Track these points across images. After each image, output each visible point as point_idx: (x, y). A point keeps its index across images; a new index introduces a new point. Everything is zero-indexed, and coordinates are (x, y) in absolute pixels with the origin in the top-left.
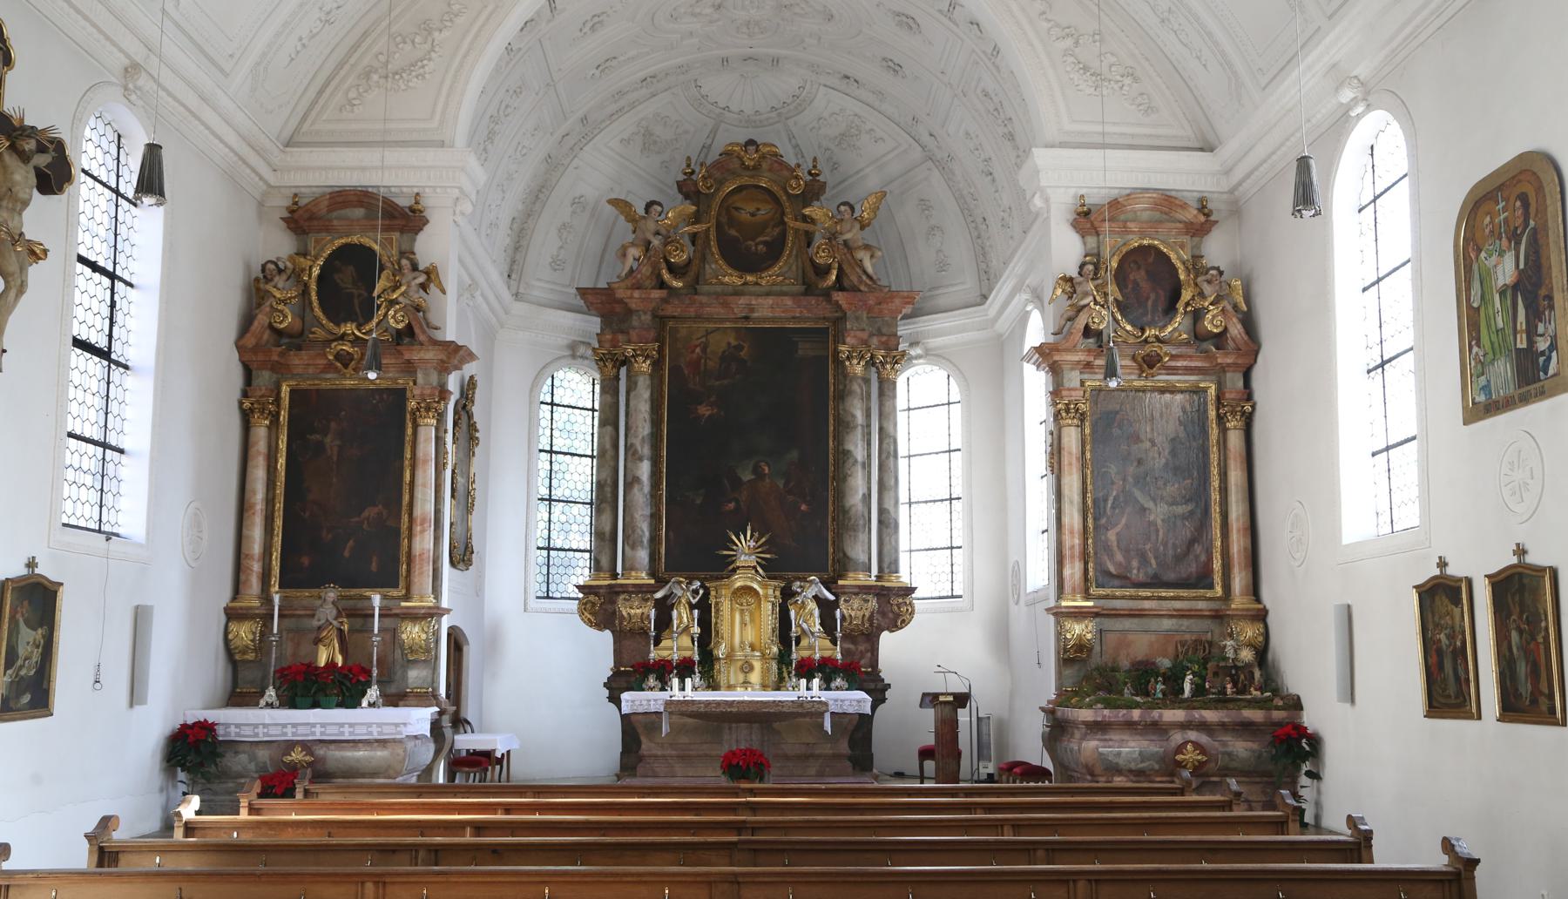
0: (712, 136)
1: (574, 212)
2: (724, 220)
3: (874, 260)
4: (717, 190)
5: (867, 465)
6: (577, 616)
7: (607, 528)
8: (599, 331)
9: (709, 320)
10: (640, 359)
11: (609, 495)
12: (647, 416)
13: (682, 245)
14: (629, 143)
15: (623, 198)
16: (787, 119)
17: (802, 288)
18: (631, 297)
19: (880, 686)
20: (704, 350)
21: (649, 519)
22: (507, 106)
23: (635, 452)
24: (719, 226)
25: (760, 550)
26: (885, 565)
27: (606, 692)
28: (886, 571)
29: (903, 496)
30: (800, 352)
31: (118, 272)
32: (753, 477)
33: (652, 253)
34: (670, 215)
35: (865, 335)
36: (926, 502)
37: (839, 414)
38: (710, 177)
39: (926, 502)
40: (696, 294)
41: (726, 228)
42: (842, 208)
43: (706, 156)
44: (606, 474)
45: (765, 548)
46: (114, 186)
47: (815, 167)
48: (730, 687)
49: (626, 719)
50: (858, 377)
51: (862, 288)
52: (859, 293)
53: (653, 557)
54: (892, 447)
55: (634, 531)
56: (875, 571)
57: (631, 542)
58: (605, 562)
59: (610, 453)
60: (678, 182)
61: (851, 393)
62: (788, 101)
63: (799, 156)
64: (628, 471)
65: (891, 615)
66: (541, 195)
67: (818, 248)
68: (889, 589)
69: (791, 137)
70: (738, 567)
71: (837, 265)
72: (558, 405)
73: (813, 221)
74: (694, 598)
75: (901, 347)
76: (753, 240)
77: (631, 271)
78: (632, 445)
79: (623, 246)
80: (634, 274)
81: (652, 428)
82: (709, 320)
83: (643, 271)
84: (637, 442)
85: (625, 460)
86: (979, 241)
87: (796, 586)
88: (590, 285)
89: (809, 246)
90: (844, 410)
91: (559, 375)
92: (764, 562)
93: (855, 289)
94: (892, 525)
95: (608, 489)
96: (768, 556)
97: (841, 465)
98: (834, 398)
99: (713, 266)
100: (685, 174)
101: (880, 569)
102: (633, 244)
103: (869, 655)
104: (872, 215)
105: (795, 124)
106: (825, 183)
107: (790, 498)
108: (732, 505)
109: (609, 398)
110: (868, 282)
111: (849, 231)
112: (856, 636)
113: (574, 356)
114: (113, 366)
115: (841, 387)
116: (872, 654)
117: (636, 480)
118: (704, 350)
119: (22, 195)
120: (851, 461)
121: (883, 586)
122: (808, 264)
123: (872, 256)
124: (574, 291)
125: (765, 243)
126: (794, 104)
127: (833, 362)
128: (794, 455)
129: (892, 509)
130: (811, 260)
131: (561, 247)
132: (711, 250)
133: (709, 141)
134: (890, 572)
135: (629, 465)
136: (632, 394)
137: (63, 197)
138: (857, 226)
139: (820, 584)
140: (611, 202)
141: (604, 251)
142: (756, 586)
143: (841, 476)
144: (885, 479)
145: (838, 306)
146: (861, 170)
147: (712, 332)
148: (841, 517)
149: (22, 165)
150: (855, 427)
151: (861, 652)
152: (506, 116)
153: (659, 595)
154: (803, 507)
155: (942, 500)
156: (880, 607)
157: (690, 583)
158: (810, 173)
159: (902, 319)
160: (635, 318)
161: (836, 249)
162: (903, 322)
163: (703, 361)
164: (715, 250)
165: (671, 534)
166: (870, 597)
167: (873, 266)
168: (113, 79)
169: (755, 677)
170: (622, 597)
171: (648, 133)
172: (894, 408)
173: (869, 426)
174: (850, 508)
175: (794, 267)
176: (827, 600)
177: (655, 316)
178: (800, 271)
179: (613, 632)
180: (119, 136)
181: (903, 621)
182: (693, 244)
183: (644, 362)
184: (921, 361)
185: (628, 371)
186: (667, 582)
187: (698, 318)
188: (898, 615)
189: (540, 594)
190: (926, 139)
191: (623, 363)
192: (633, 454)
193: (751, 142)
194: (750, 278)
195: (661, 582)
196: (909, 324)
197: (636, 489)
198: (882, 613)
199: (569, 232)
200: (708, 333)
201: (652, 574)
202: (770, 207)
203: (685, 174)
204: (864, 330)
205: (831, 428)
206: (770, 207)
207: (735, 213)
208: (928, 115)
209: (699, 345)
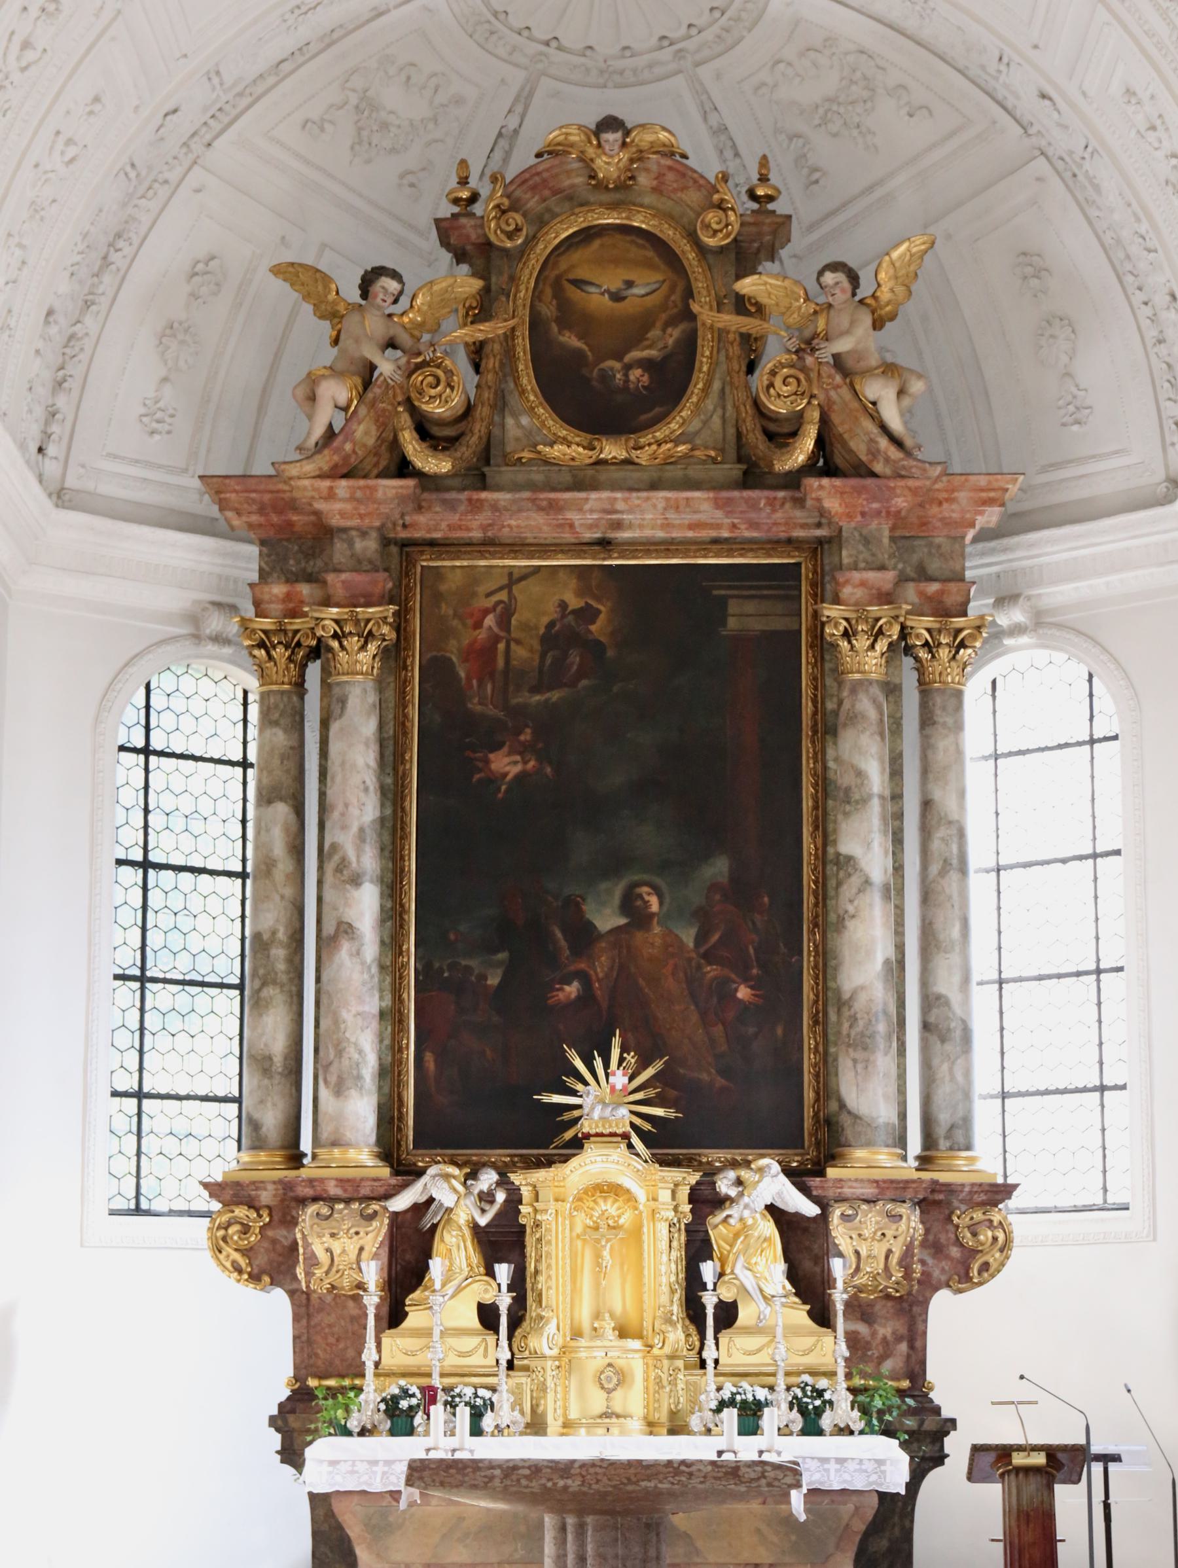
0: (519, 109)
1: (194, 296)
2: (548, 310)
3: (906, 401)
4: (531, 240)
5: (894, 891)
6: (208, 1254)
7: (278, 1045)
8: (254, 577)
9: (517, 548)
10: (353, 642)
11: (281, 966)
12: (371, 780)
13: (449, 373)
14: (322, 130)
15: (309, 260)
16: (698, 64)
17: (735, 471)
18: (331, 495)
19: (930, 1424)
20: (504, 621)
21: (375, 1024)
22: (26, 45)
23: (343, 865)
24: (536, 325)
25: (639, 1096)
26: (940, 1131)
27: (275, 1440)
28: (943, 1144)
29: (982, 964)
30: (732, 623)
32: (622, 921)
33: (377, 391)
34: (419, 301)
35: (885, 579)
36: (1040, 978)
37: (825, 768)
38: (515, 206)
39: (1040, 978)
40: (484, 487)
41: (555, 328)
42: (829, 278)
43: (506, 160)
44: (274, 918)
45: (651, 1093)
47: (764, 179)
48: (568, 1426)
49: (319, 1502)
50: (870, 682)
51: (878, 467)
52: (869, 482)
53: (388, 1118)
54: (955, 848)
55: (340, 1053)
56: (915, 1145)
57: (333, 1079)
58: (271, 1119)
59: (284, 865)
60: (438, 222)
61: (854, 718)
62: (700, 22)
63: (729, 154)
64: (326, 909)
65: (955, 1252)
66: (114, 257)
67: (773, 373)
68: (949, 1188)
69: (708, 109)
70: (587, 1136)
71: (816, 415)
72: (161, 754)
73: (759, 310)
74: (483, 1211)
75: (974, 609)
76: (619, 357)
77: (330, 434)
78: (334, 847)
79: (309, 374)
80: (336, 443)
81: (382, 805)
82: (517, 548)
84: (345, 840)
85: (320, 883)
86: (1163, 349)
87: (725, 1185)
88: (238, 471)
89: (751, 368)
90: (836, 759)
91: (163, 682)
92: (647, 1126)
93: (863, 471)
94: (957, 1034)
95: (279, 954)
96: (659, 1112)
97: (831, 893)
98: (815, 732)
99: (525, 420)
100: (456, 201)
101: (929, 1140)
102: (334, 371)
103: (903, 1347)
104: (900, 290)
105: (718, 76)
106: (789, 217)
107: (711, 971)
108: (572, 990)
109: (280, 738)
110: (894, 453)
111: (847, 332)
112: (871, 1304)
113: (197, 638)
115: (830, 705)
116: (912, 1347)
117: (346, 929)
118: (504, 621)
120: (855, 881)
121: (935, 1182)
122: (748, 411)
123: (901, 393)
124: (197, 483)
125: (647, 365)
126: (715, 29)
127: (812, 646)
128: (718, 868)
129: (954, 997)
130: (757, 404)
131: (165, 380)
132: (517, 380)
133: (513, 123)
134: (951, 1149)
135: (328, 895)
136: (335, 727)
138: (867, 320)
139: (783, 1178)
140: (278, 270)
141: (265, 392)
142: (628, 1182)
143: (832, 917)
144: (938, 925)
145: (822, 512)
146: (880, 183)
147: (523, 578)
148: (833, 1017)
150: (865, 801)
151: (885, 1339)
152: (24, 69)
153: (401, 1203)
154: (743, 993)
155: (1078, 974)
156: (927, 1231)
157: (473, 1175)
158: (752, 195)
159: (976, 540)
160: (339, 546)
161: (813, 375)
162: (980, 546)
163: (501, 646)
164: (528, 380)
165: (429, 1058)
166: (903, 1209)
167: (906, 414)
169: (633, 1400)
170: (312, 1209)
171: (367, 105)
172: (959, 753)
173: (897, 797)
174: (855, 993)
175: (716, 421)
176: (797, 1215)
177: (386, 542)
178: (731, 431)
179: (292, 1294)
181: (985, 1266)
182: (477, 368)
183: (363, 648)
184: (1024, 640)
185: (326, 672)
186: (420, 1173)
187: (490, 545)
188: (974, 1252)
189: (121, 1204)
190: (1028, 105)
191: (316, 652)
192: (339, 870)
193: (610, 123)
194: (612, 450)
195: (408, 1173)
196: (992, 552)
197: (344, 952)
198: (933, 1245)
199: (182, 342)
200: (514, 579)
201: (388, 1150)
202: (659, 277)
203: (456, 201)
204: (882, 568)
205: (807, 804)
206: (659, 277)
207: (573, 293)
208: (1036, 47)
209: (494, 609)
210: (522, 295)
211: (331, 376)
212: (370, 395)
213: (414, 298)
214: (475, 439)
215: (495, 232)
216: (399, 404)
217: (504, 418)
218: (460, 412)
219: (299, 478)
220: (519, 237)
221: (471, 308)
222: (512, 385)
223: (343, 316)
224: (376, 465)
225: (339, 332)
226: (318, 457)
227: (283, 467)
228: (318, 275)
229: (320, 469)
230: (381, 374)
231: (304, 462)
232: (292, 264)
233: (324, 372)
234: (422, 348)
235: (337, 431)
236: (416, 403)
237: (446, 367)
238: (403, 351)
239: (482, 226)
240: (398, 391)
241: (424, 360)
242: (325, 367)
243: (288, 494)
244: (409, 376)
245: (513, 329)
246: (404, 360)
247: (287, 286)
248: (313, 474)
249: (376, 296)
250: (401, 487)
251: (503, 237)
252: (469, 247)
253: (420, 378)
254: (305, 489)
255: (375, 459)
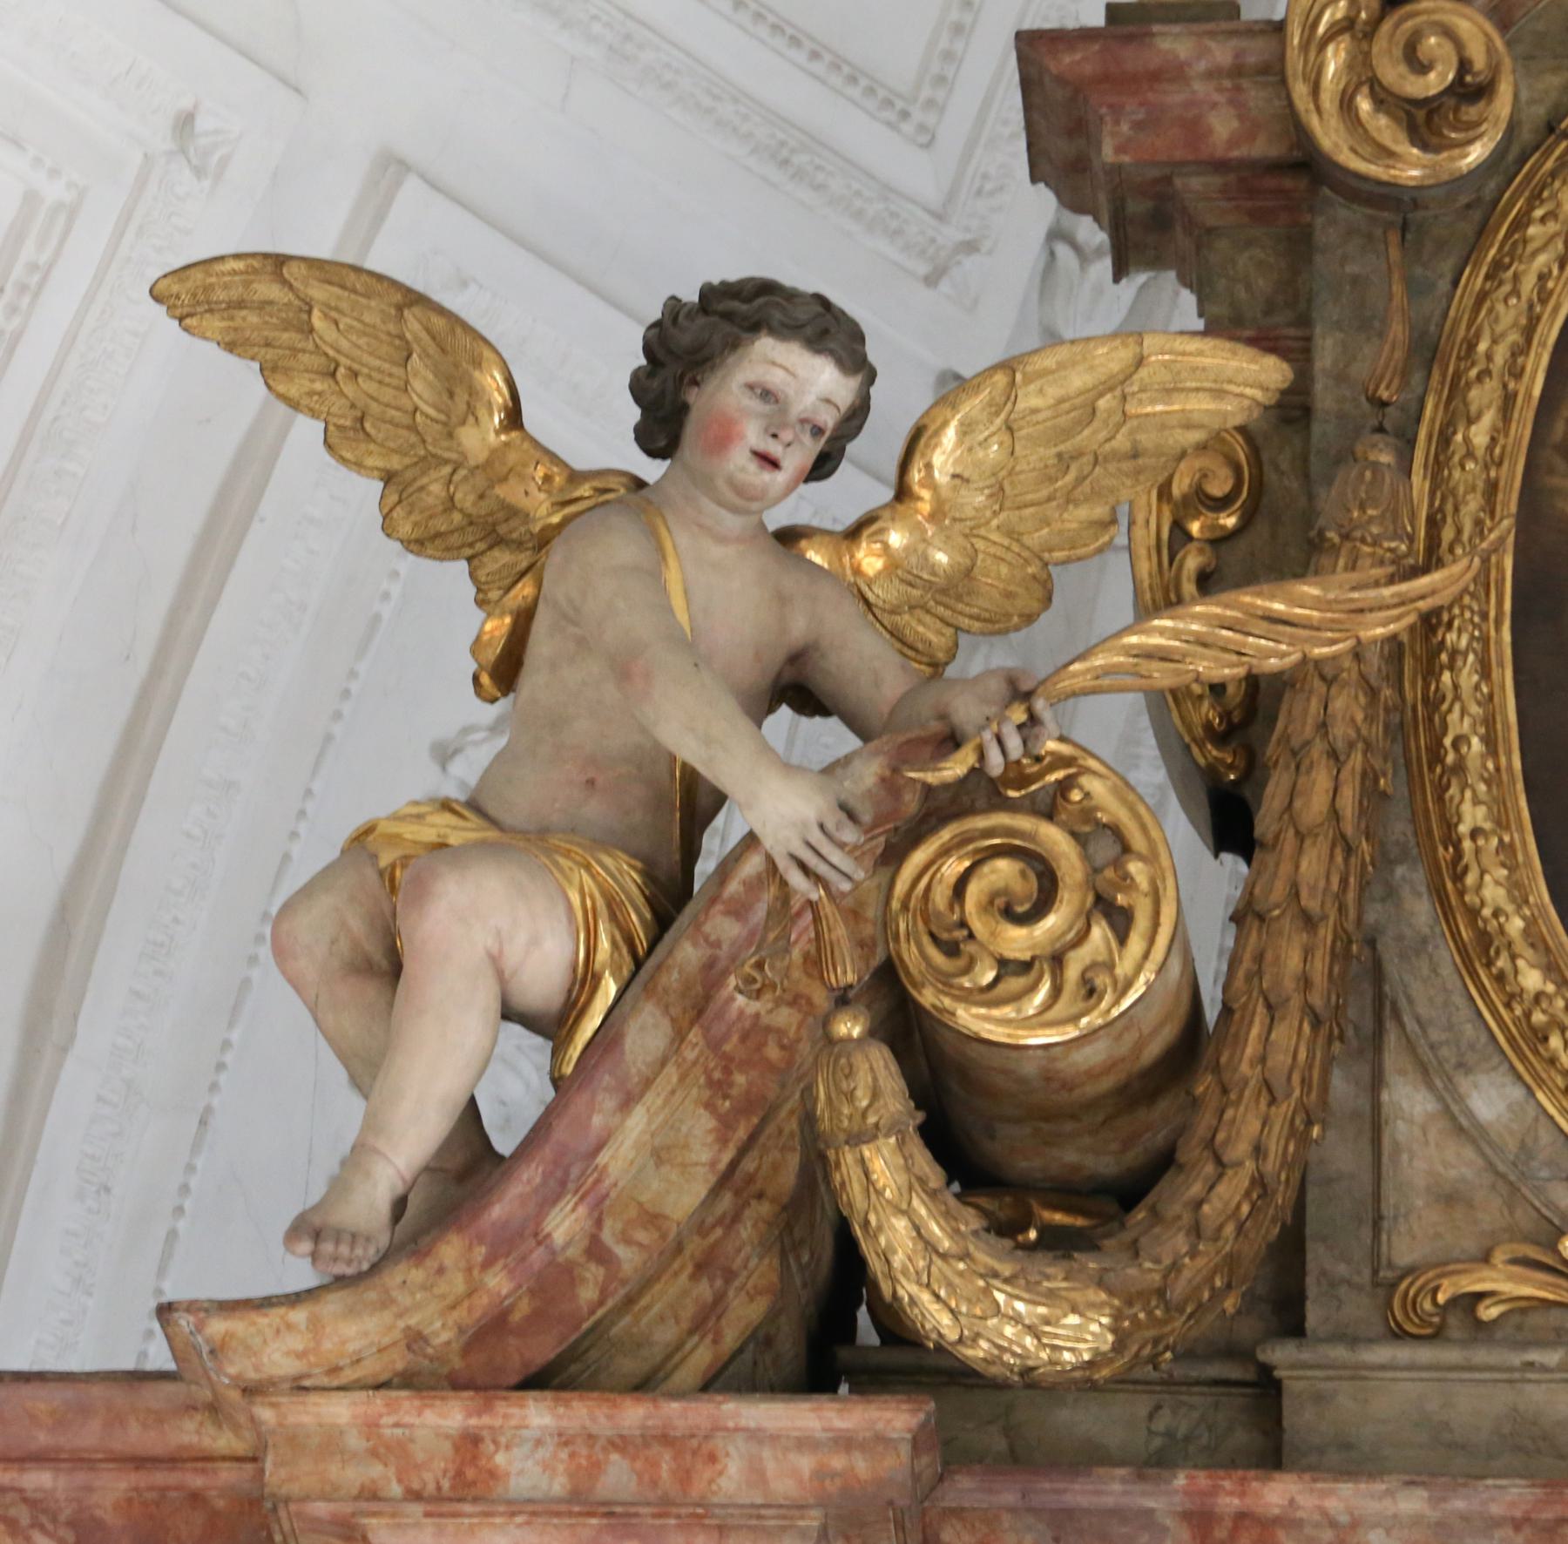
34: (944, 455)
80: (502, 1208)
83: (618, 1159)
210: (1480, 435)
211: (482, 847)
212: (685, 953)
213: (917, 440)
214: (1231, 1191)
215: (1347, 104)
216: (843, 1000)
217: (1377, 1082)
218: (1153, 1050)
219: (299, 1387)
220: (1472, 131)
221: (1201, 500)
222: (1421, 911)
223: (544, 540)
224: (706, 1319)
225: (524, 621)
226: (406, 1274)
227: (218, 1326)
228: (413, 323)
229: (415, 1339)
230: (751, 840)
231: (332, 1304)
232: (279, 262)
233: (439, 826)
234: (966, 711)
235: (504, 1144)
236: (928, 997)
237: (1087, 813)
238: (863, 732)
239: (1274, 72)
240: (839, 932)
241: (978, 771)
242: (446, 806)
243: (228, 1475)
244: (893, 856)
245: (1430, 623)
246: (868, 773)
247: (245, 375)
248: (372, 1368)
249: (723, 439)
250: (845, 1442)
251: (1383, 127)
252: (1194, 185)
253: (953, 868)
254: (330, 1444)
255: (704, 1290)
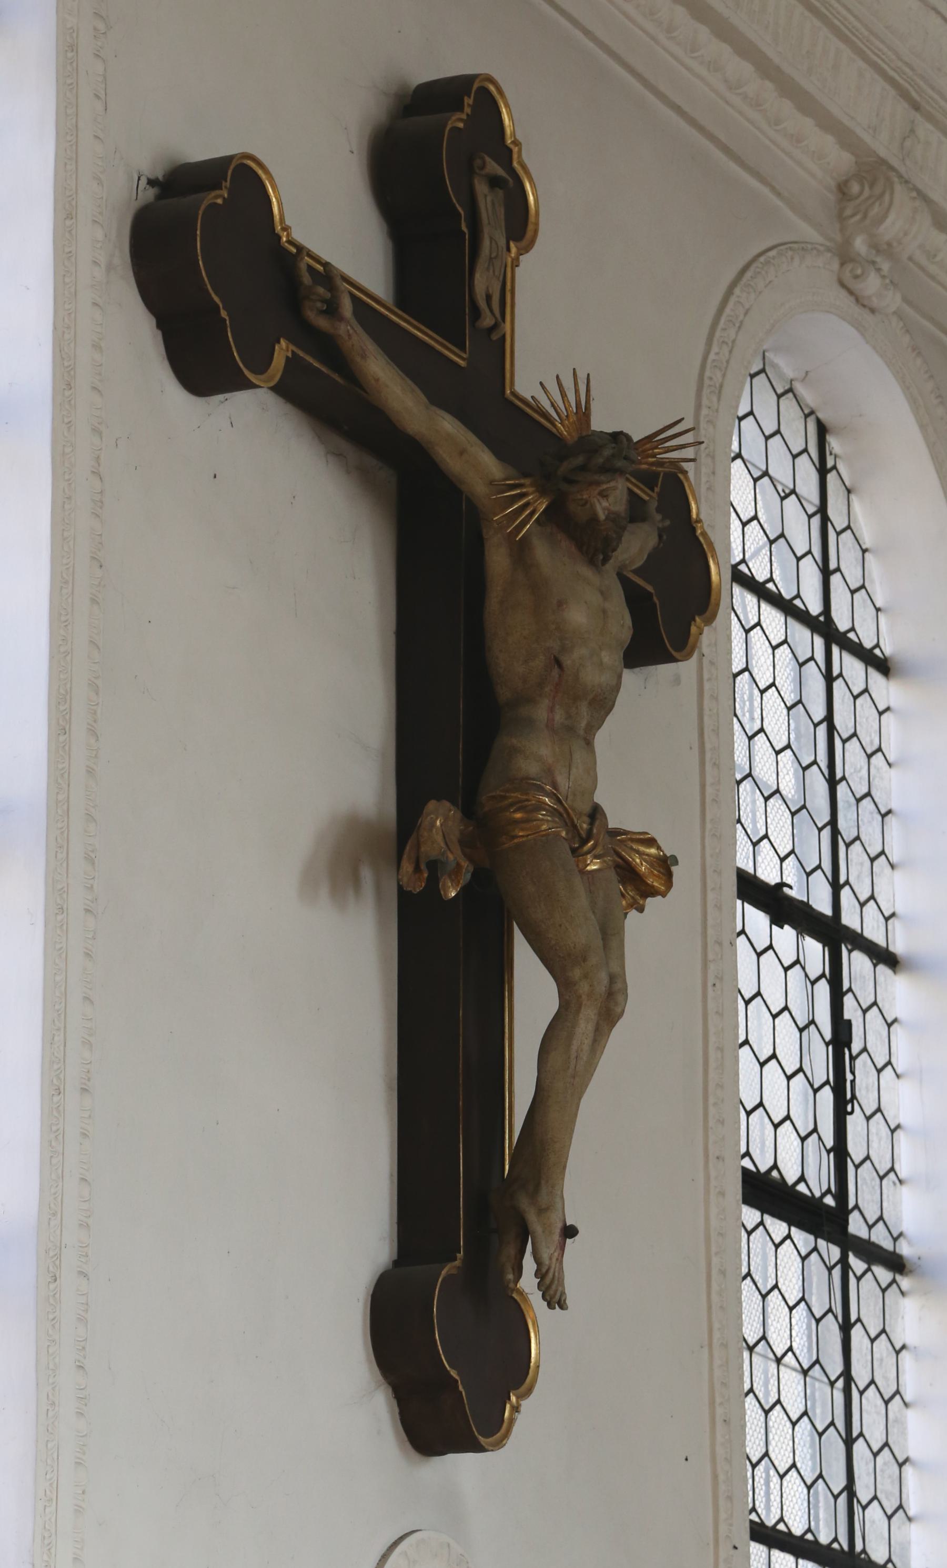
31: (849, 919)
46: (815, 608)
114: (857, 1265)
119: (593, 677)
137: (686, 668)
149: (586, 571)
168: (809, 233)
180: (822, 430)
